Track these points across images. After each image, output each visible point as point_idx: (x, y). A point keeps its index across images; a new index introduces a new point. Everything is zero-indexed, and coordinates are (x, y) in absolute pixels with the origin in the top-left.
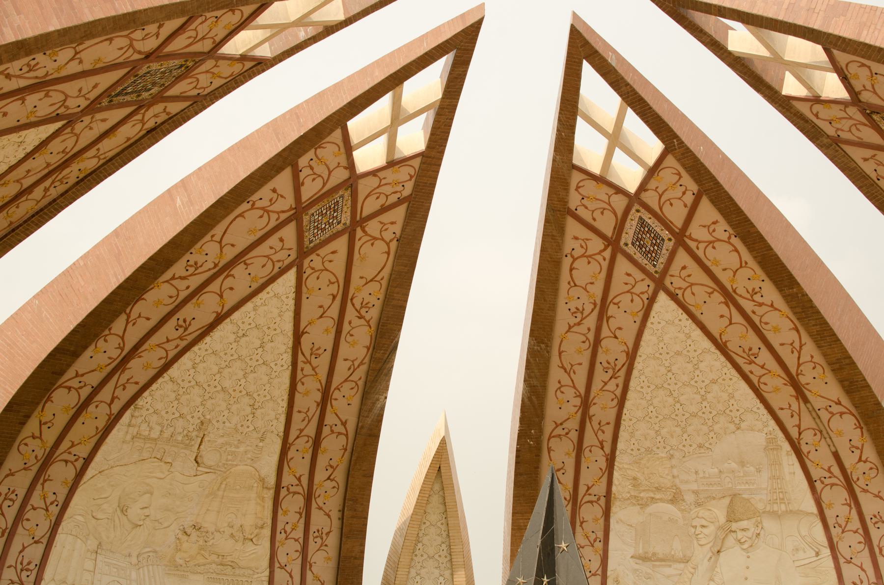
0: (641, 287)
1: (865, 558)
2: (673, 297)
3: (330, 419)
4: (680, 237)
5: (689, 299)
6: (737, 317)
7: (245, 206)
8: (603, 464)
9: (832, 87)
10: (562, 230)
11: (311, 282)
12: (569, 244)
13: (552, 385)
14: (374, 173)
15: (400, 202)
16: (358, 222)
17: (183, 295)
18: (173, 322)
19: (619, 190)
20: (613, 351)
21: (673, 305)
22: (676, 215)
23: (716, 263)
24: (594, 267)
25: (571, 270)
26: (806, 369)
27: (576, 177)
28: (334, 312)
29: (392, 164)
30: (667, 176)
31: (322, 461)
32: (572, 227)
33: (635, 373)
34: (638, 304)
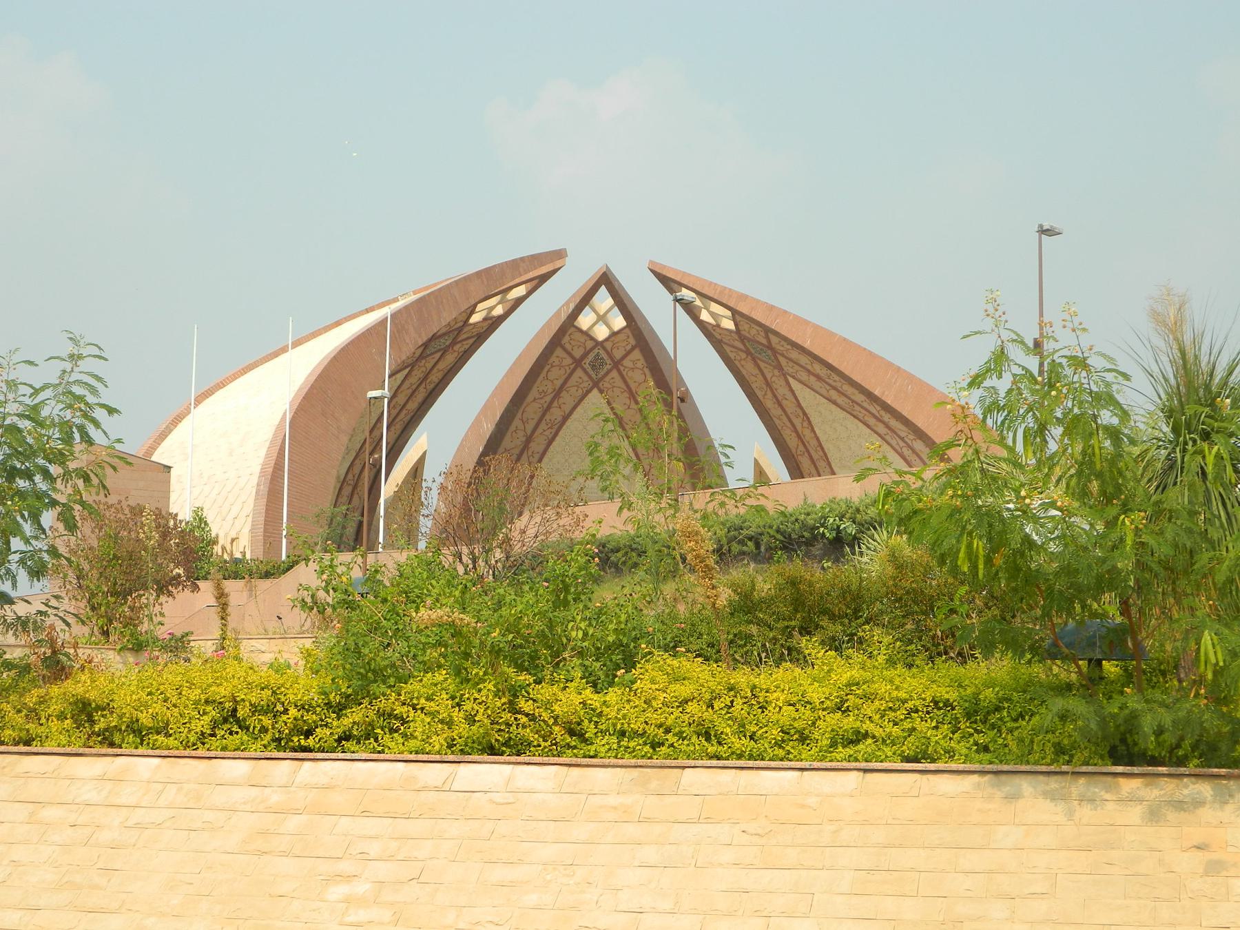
0: (586, 384)
4: (617, 364)
9: (728, 324)
10: (552, 353)
11: (414, 373)
12: (553, 359)
13: (513, 428)
14: (475, 324)
16: (454, 343)
19: (592, 339)
20: (556, 414)
22: (618, 354)
24: (562, 371)
27: (572, 329)
29: (485, 319)
30: (622, 337)
32: (559, 352)
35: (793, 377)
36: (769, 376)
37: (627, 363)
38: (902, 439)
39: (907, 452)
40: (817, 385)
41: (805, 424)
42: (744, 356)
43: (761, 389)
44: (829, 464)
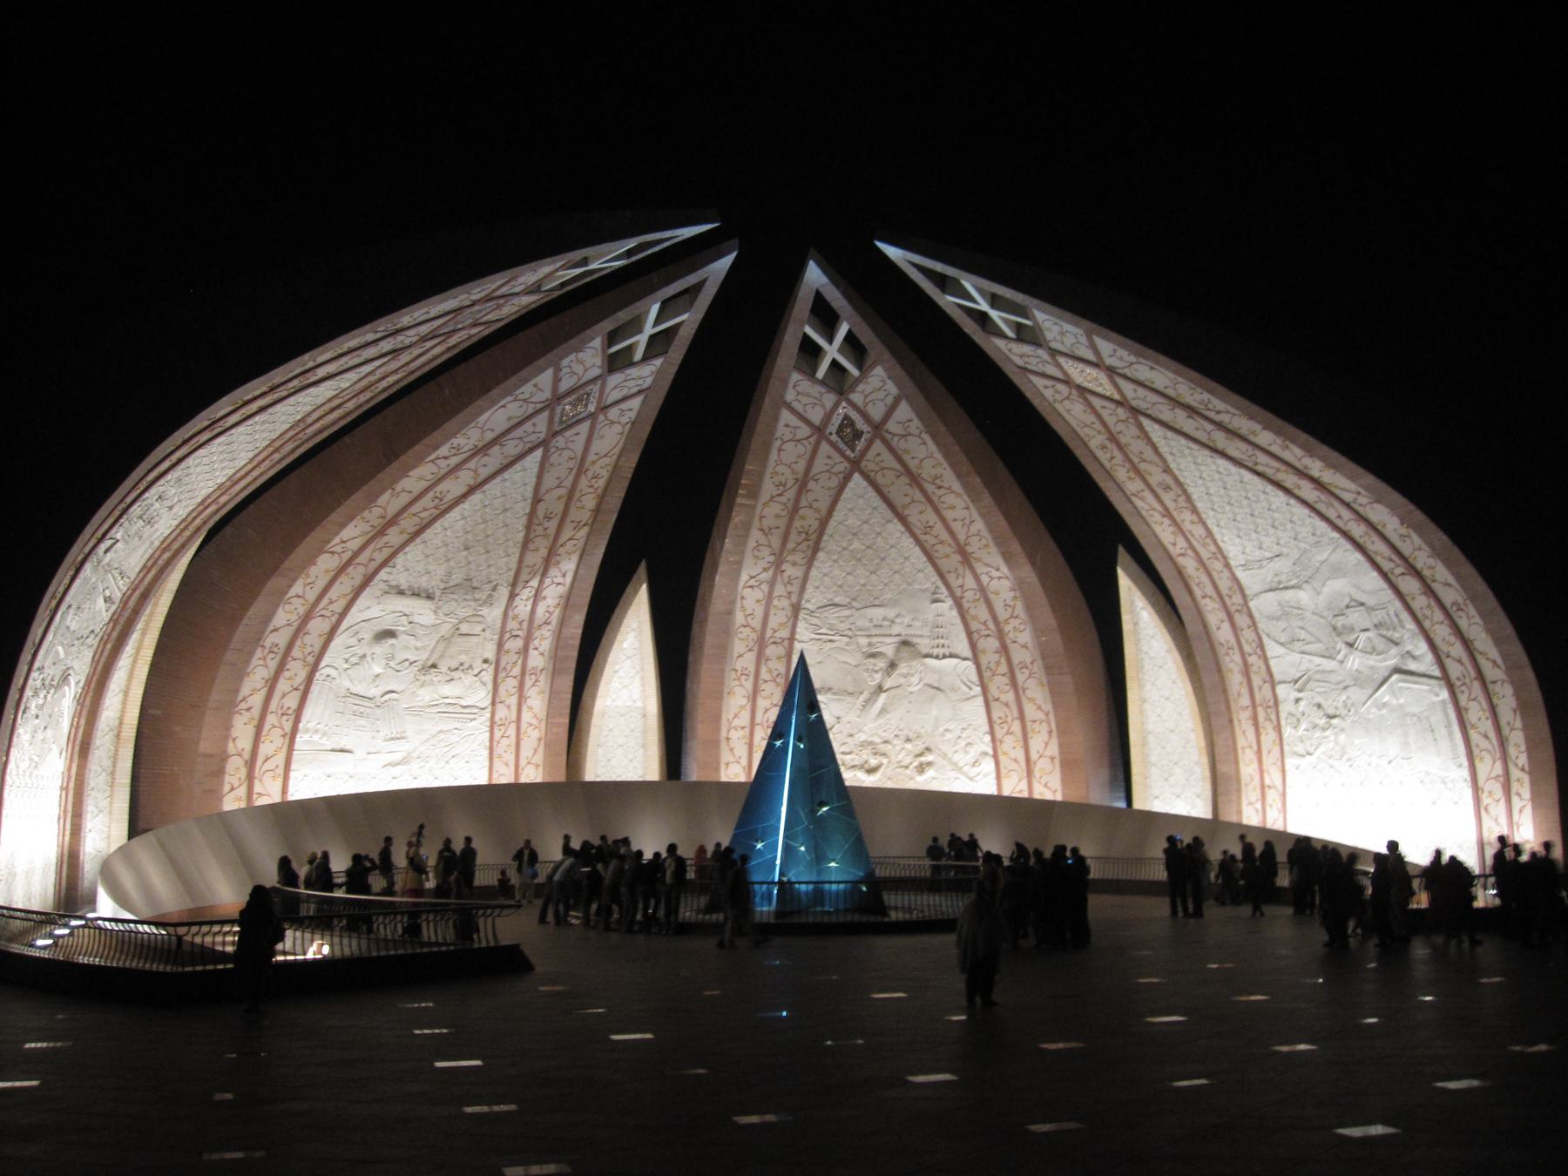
1: (1009, 697)
2: (866, 477)
3: (553, 572)
4: (878, 428)
5: (880, 480)
6: (918, 496)
7: (510, 398)
8: (789, 612)
11: (554, 458)
12: (781, 430)
13: (751, 544)
15: (640, 392)
16: (604, 409)
17: (442, 472)
18: (431, 495)
21: (865, 483)
22: (877, 413)
23: (907, 452)
25: (780, 450)
26: (974, 540)
28: (568, 483)
31: (541, 610)
33: (825, 538)
34: (834, 482)
35: (1149, 416)
36: (1110, 421)
37: (891, 426)
38: (1347, 505)
39: (1358, 530)
40: (1188, 425)
41: (1182, 498)
42: (1061, 387)
43: (1104, 447)
44: (1227, 566)
